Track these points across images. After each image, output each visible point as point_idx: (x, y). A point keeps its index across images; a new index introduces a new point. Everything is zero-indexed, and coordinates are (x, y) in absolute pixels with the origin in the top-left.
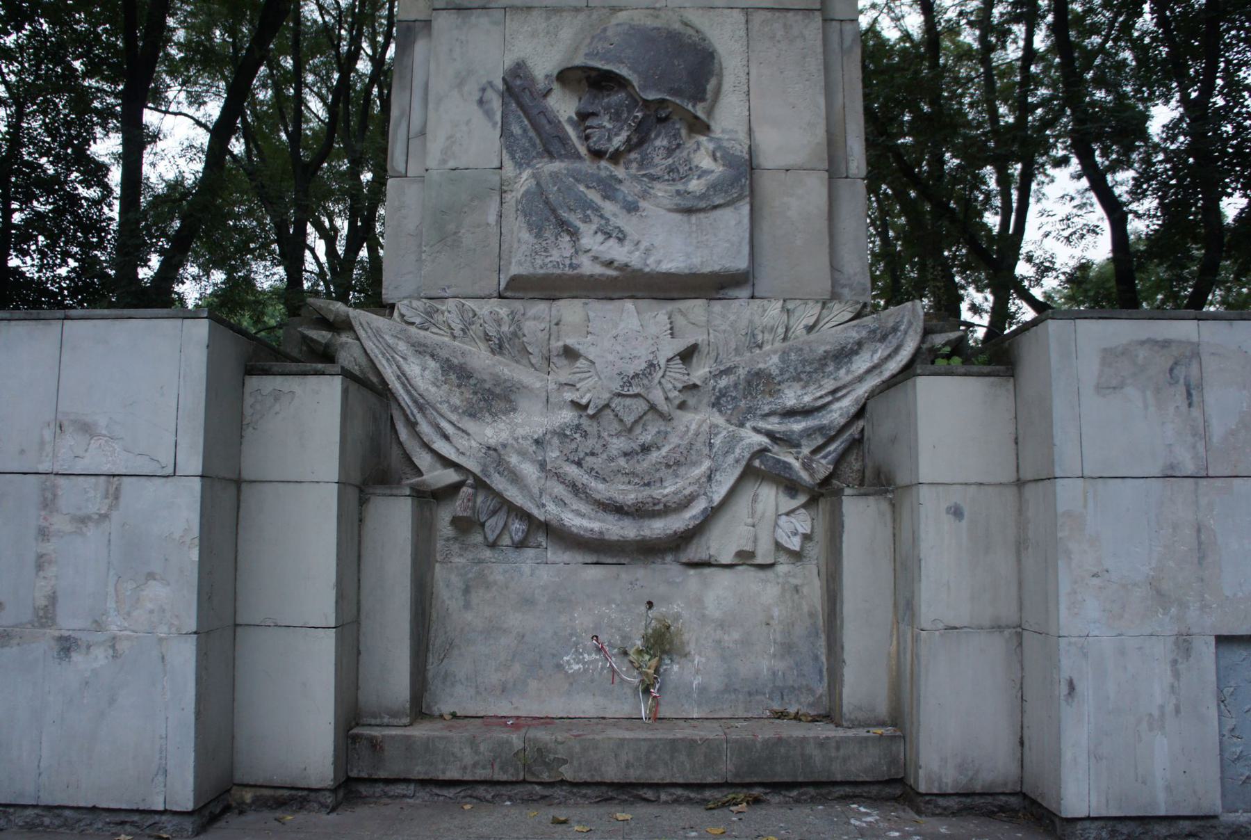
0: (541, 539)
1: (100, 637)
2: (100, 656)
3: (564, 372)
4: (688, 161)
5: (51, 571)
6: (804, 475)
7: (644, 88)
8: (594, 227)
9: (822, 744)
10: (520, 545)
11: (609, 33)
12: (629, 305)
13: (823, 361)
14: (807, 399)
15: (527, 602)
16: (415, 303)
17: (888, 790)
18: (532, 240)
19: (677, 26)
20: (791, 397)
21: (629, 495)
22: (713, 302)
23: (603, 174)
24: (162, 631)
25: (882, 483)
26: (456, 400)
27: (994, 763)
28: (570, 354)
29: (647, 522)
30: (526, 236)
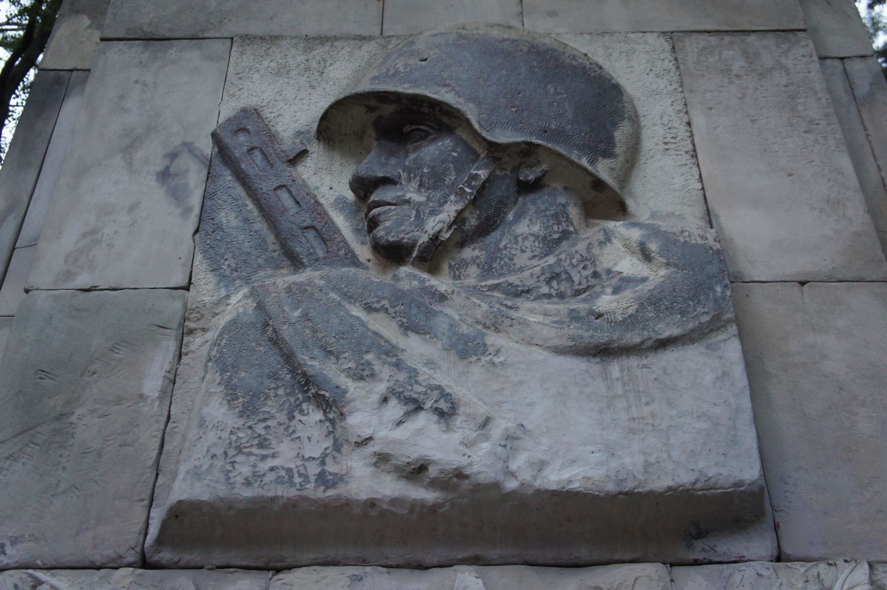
4: (588, 260)
7: (491, 126)
8: (381, 388)
18: (232, 420)
22: (679, 571)
30: (218, 411)
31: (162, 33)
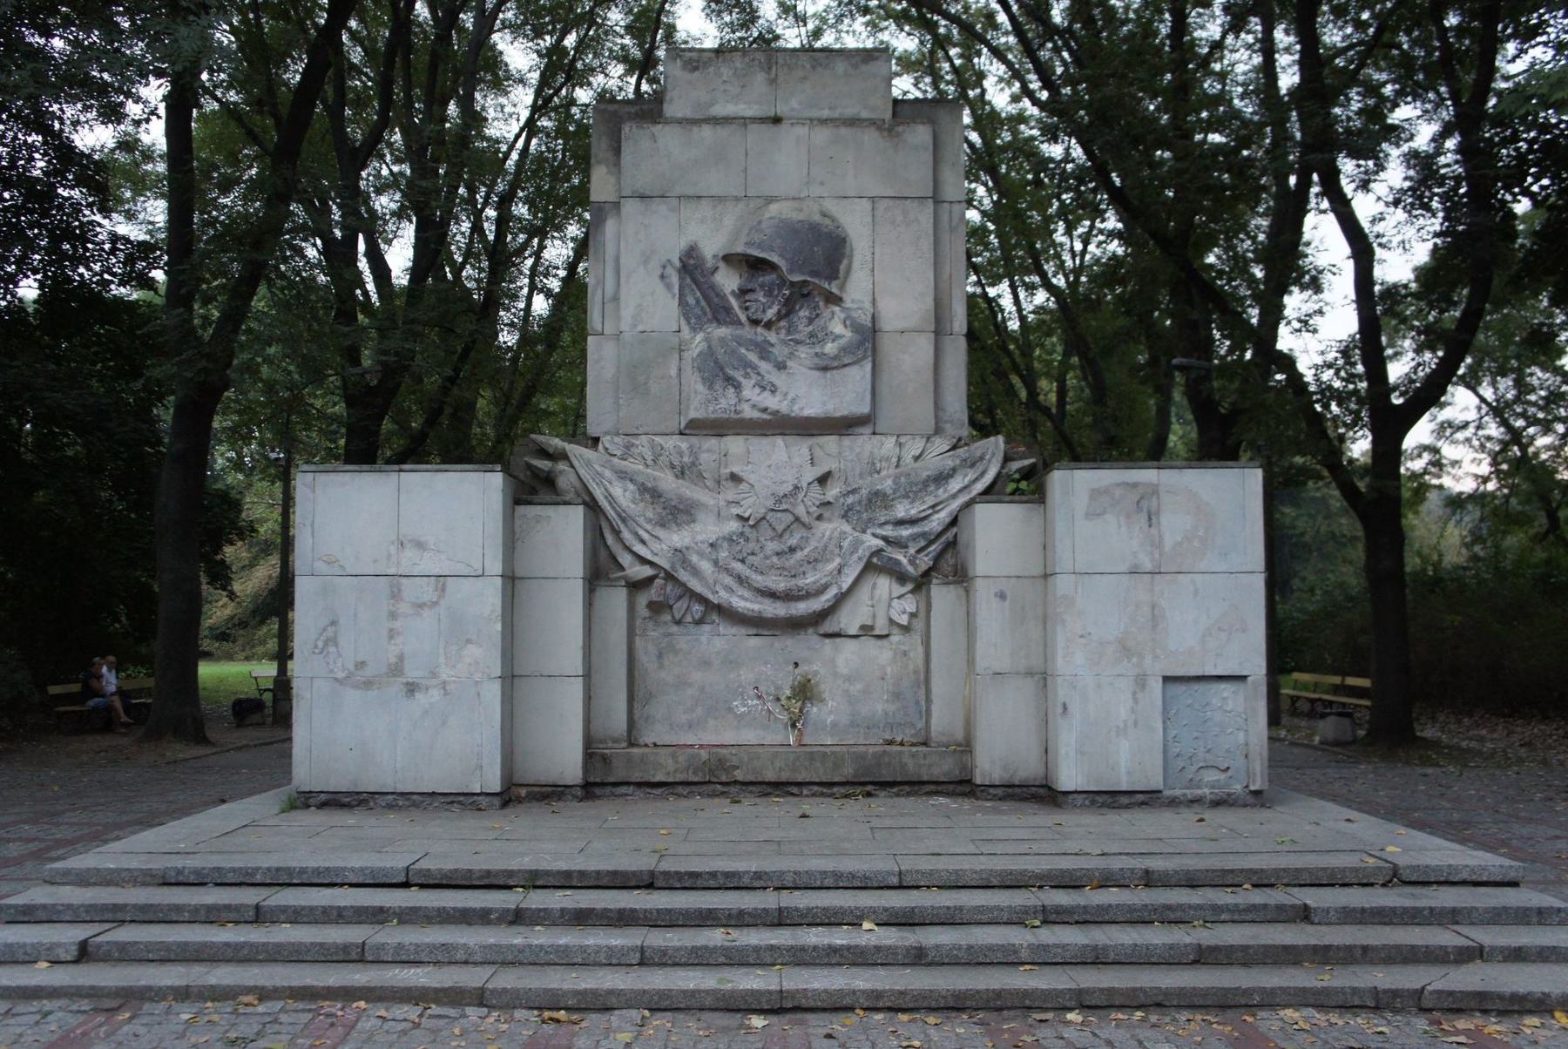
0: (715, 617)
1: (434, 682)
2: (435, 694)
3: (730, 493)
4: (824, 328)
5: (399, 640)
6: (910, 569)
7: (791, 271)
9: (913, 756)
10: (699, 622)
11: (764, 226)
12: (779, 441)
13: (926, 483)
14: (913, 512)
15: (705, 664)
16: (616, 439)
17: (960, 788)
19: (817, 218)
20: (901, 510)
21: (780, 584)
23: (760, 339)
24: (477, 677)
25: (961, 576)
26: (650, 515)
27: (1028, 768)
28: (735, 478)
29: (793, 604)
30: (700, 387)
31: (648, 193)
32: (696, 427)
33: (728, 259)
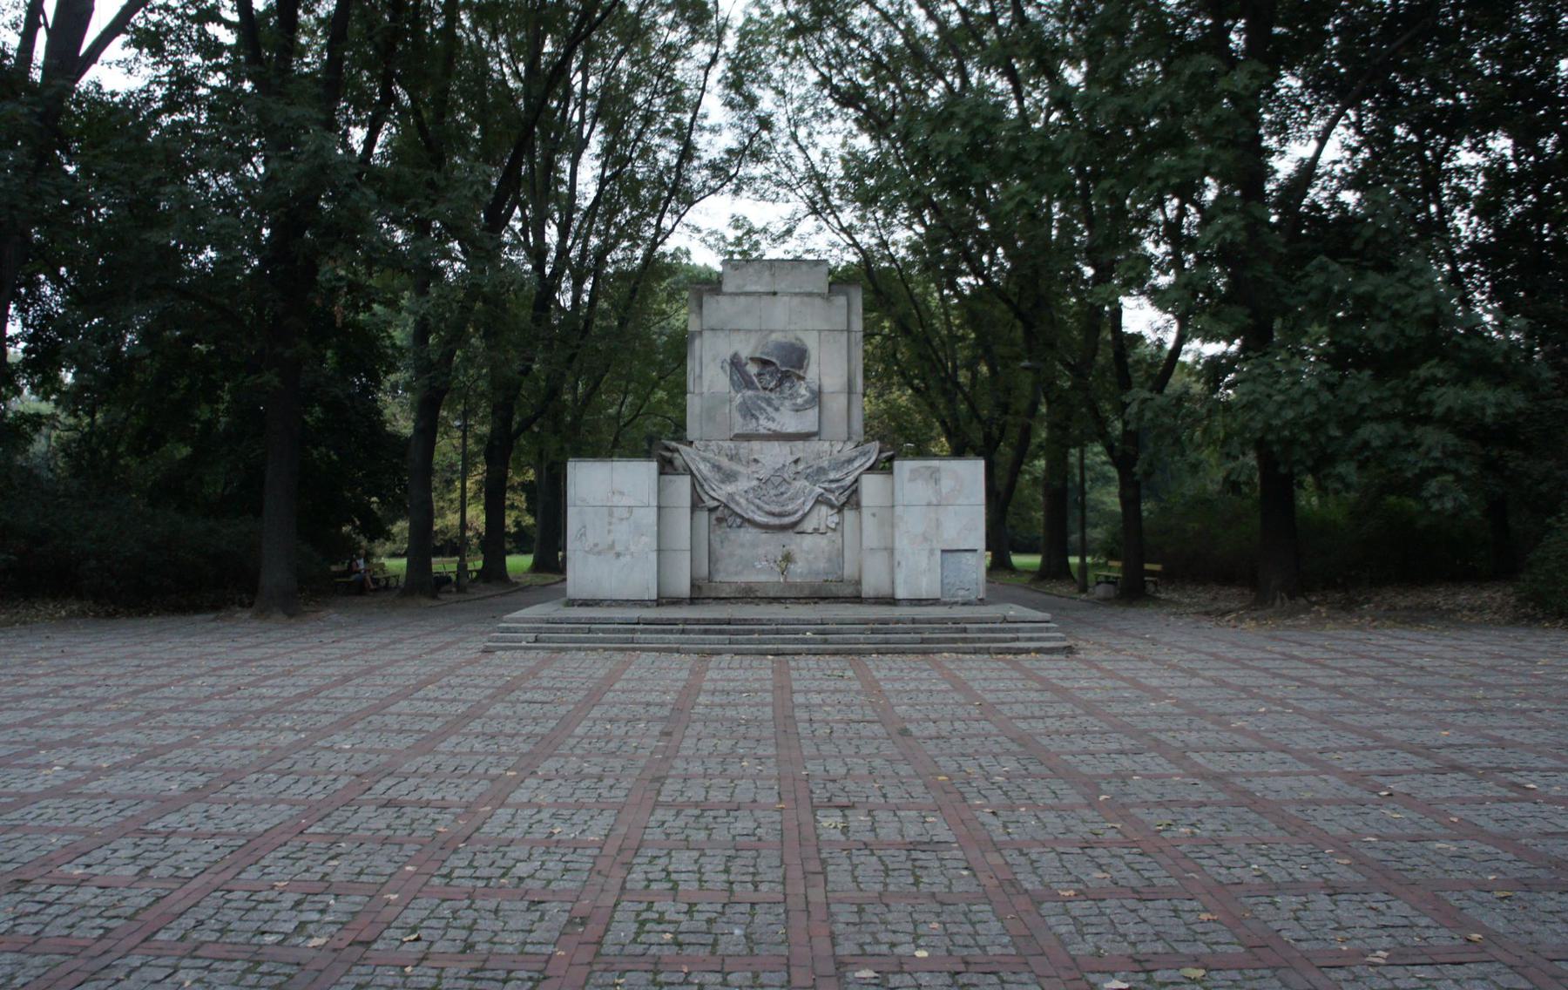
3: (754, 467)
15: (742, 546)
20: (832, 476)
21: (777, 509)
25: (858, 506)
27: (885, 591)
28: (756, 461)
32: (738, 437)
33: (752, 359)
